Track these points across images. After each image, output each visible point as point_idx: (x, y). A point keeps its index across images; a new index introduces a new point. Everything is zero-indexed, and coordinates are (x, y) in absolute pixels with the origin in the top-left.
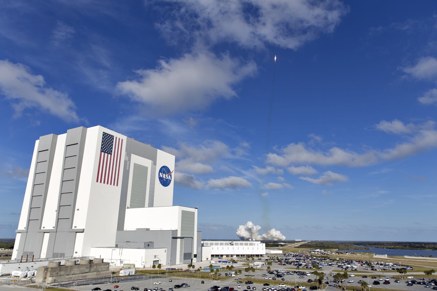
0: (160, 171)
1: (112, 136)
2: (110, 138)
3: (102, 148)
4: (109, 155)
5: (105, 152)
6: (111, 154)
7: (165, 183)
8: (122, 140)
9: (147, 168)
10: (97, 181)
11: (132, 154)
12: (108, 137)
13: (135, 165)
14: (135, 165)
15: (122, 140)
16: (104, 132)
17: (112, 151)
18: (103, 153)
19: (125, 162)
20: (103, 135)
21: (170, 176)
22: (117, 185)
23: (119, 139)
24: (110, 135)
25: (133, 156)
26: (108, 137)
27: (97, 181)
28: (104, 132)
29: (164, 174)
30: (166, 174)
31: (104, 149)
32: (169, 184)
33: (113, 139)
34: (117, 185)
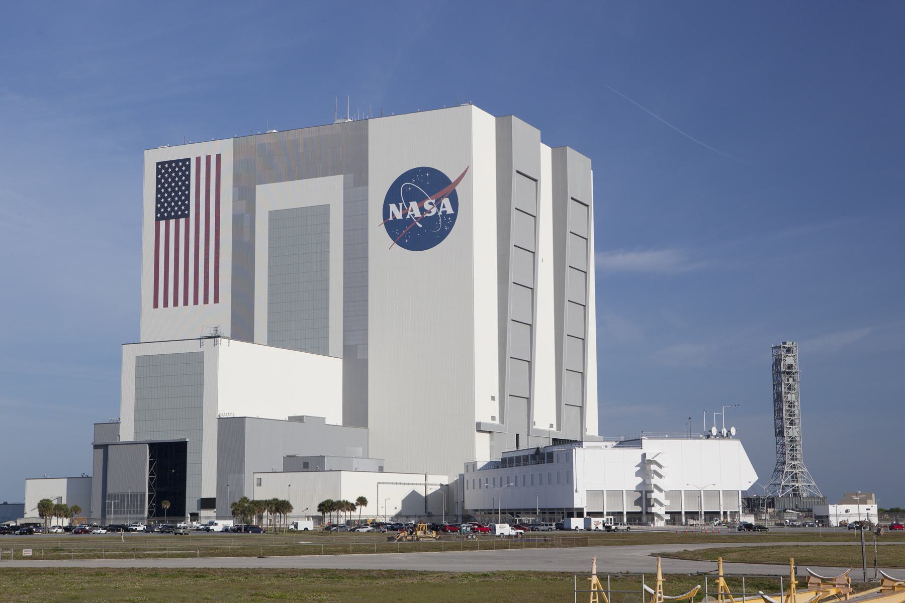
0: (393, 196)
1: (184, 161)
2: (180, 168)
3: (158, 210)
4: (182, 221)
5: (167, 219)
6: (187, 217)
7: (419, 235)
8: (218, 157)
9: (323, 211)
10: (156, 305)
11: (257, 186)
12: (173, 169)
13: (275, 216)
14: (275, 216)
15: (218, 157)
16: (158, 164)
17: (188, 207)
18: (163, 223)
19: (237, 220)
20: (158, 171)
21: (446, 201)
22: (216, 300)
23: (208, 158)
24: (177, 162)
25: (260, 189)
26: (173, 169)
27: (156, 305)
28: (158, 164)
29: (414, 205)
30: (420, 199)
31: (166, 211)
32: (444, 234)
33: (188, 168)
34: (216, 300)
